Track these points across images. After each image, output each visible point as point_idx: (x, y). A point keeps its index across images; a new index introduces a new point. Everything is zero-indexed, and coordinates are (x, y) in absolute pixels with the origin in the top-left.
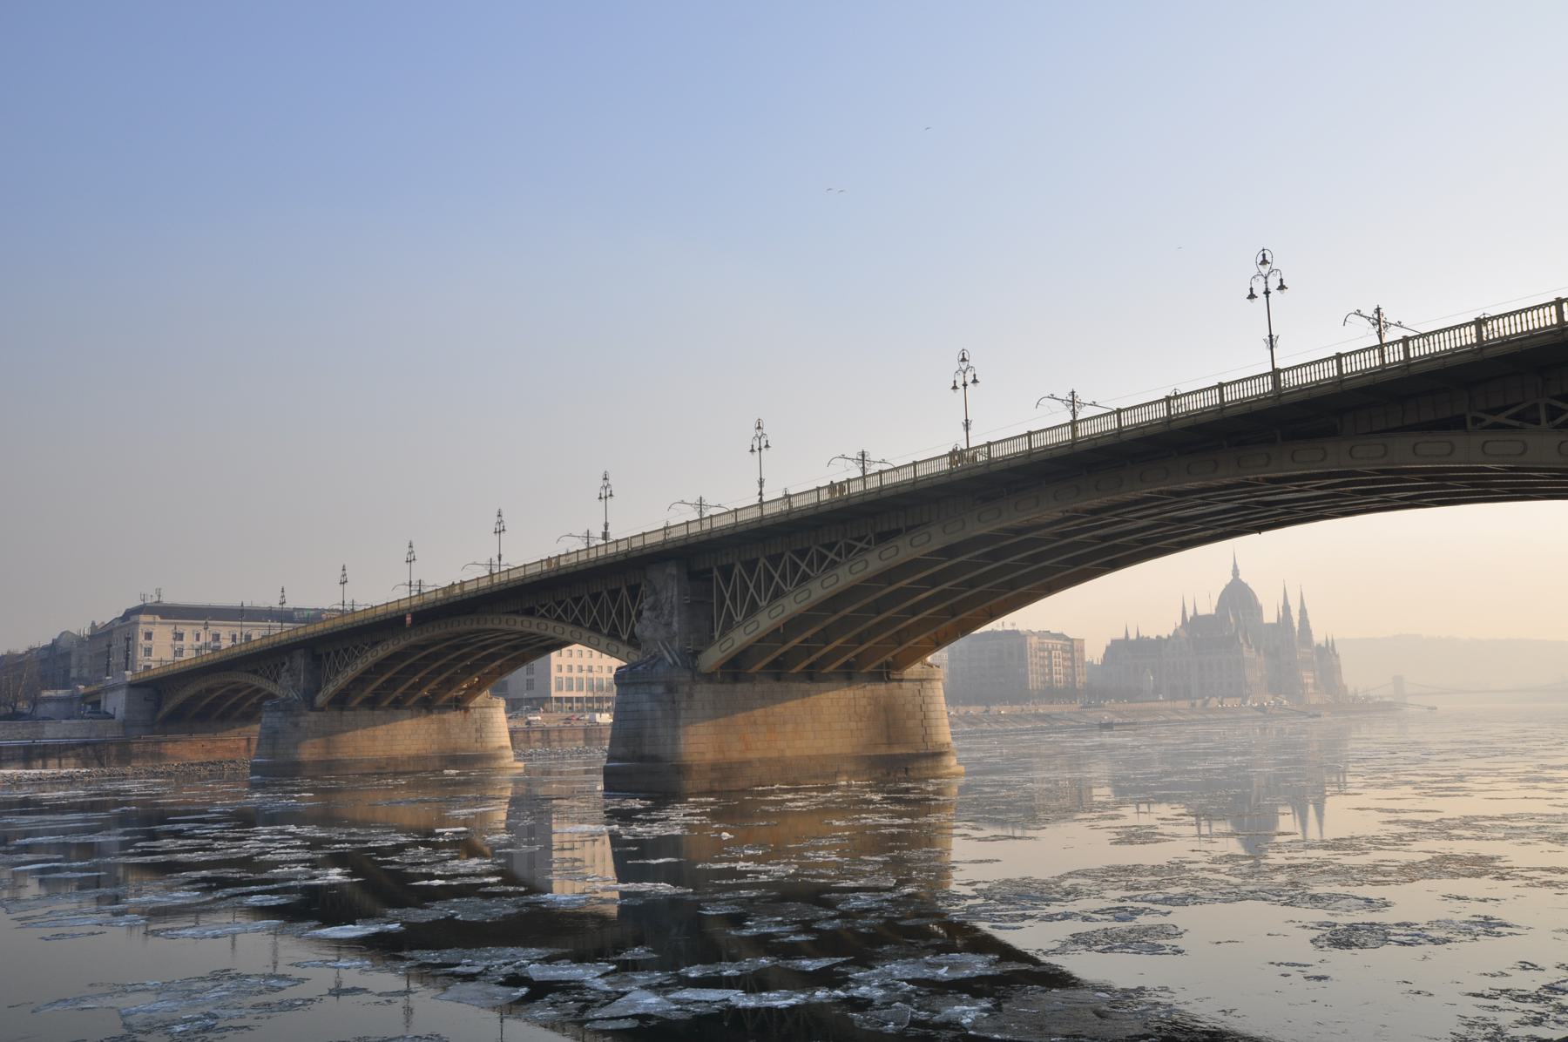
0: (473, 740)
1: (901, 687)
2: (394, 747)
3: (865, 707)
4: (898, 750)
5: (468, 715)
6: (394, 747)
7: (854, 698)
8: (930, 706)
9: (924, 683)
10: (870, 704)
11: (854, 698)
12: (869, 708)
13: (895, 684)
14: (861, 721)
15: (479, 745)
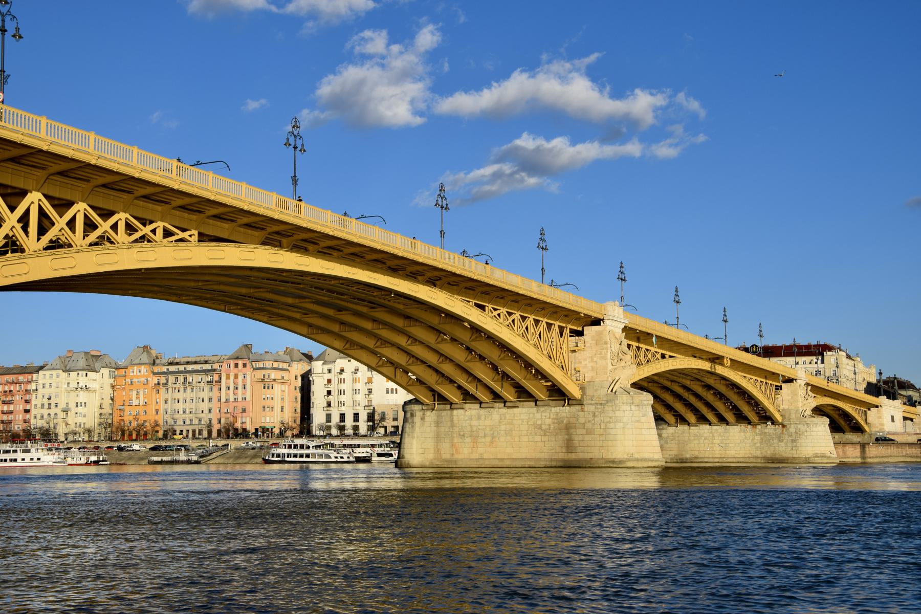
0: (790, 449)
1: (583, 410)
2: (727, 452)
3: (549, 425)
4: (573, 456)
5: (784, 429)
6: (727, 452)
7: (542, 418)
8: (608, 425)
9: (606, 408)
10: (554, 423)
11: (542, 418)
12: (552, 426)
13: (577, 407)
14: (545, 435)
15: (794, 452)
